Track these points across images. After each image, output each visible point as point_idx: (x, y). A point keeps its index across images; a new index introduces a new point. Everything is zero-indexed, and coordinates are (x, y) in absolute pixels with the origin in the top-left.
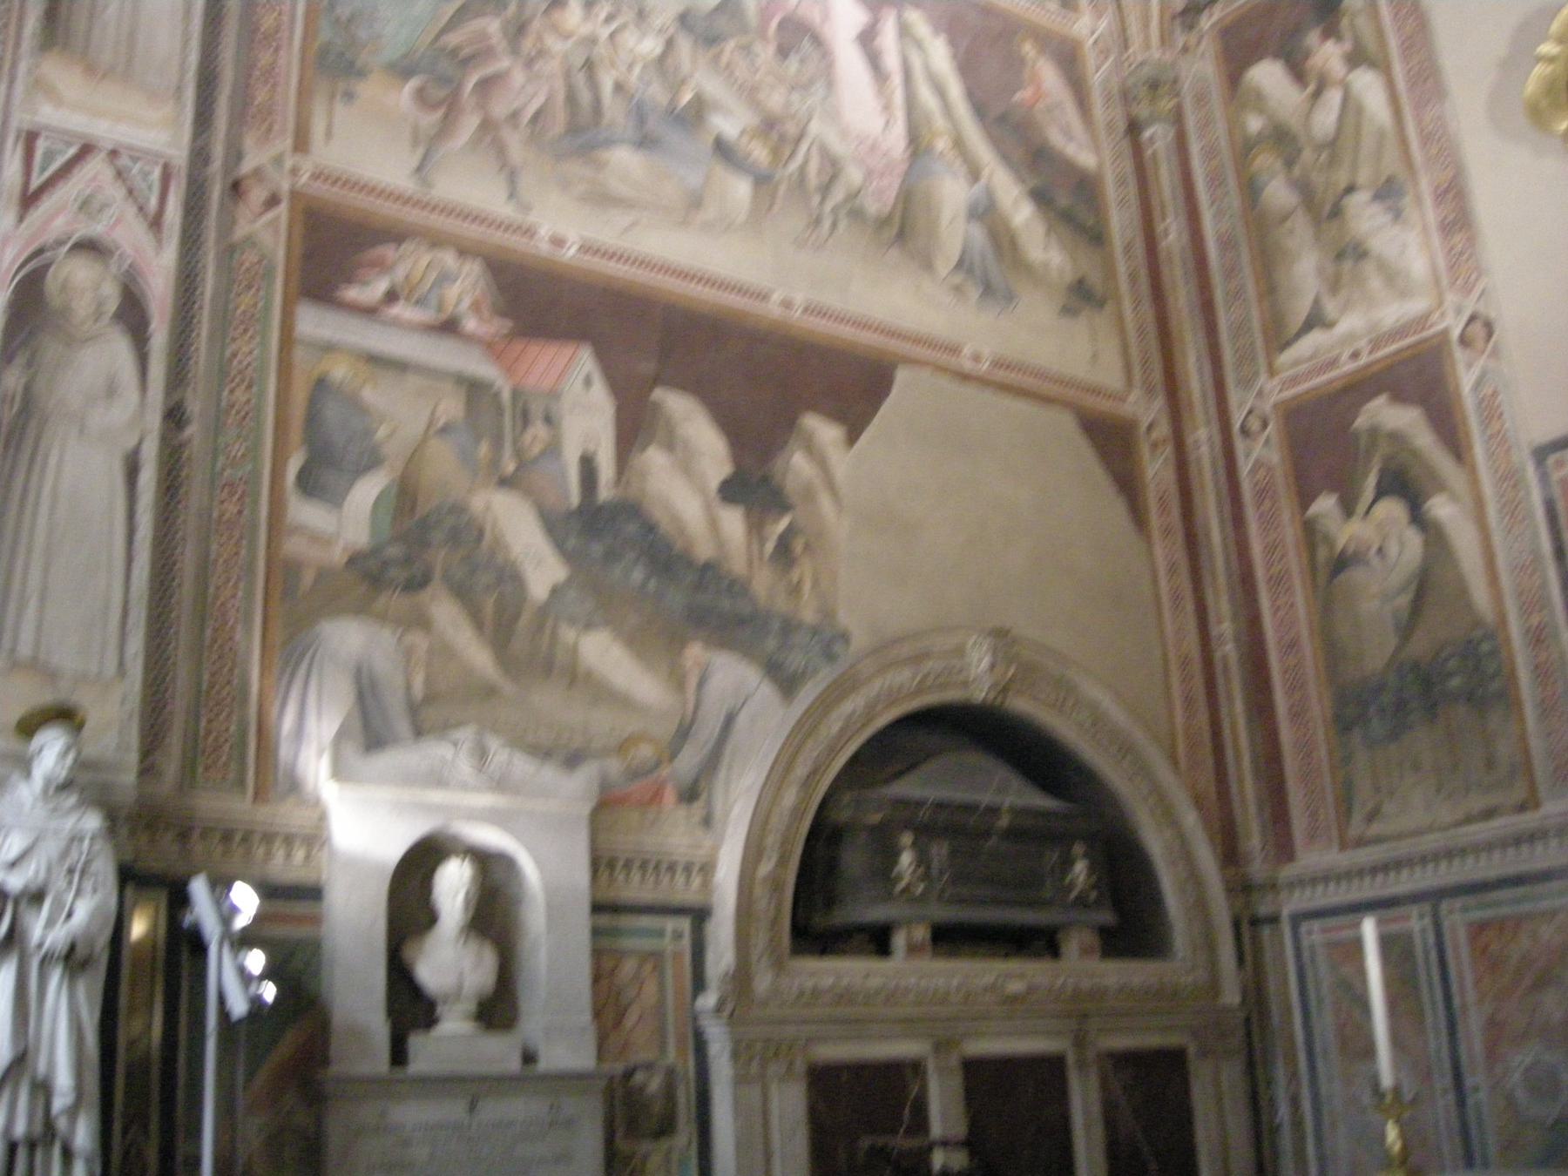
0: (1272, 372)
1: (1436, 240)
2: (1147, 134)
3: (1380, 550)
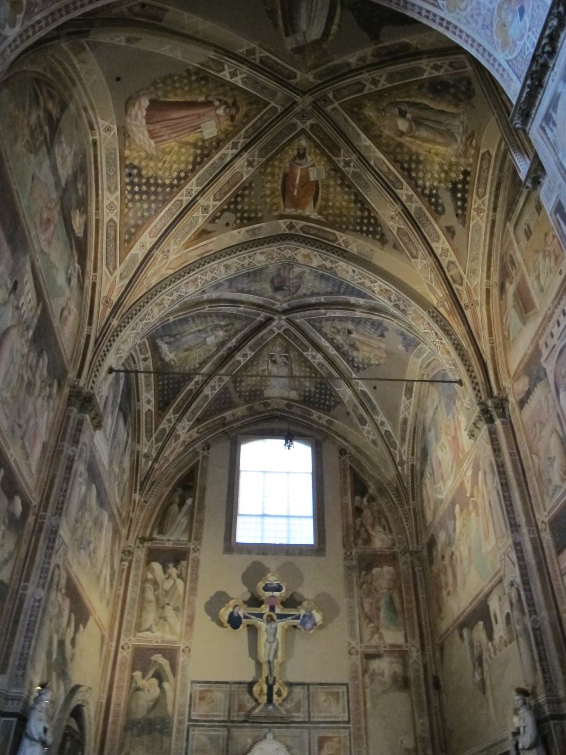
0: (135, 636)
1: (184, 626)
2: (123, 563)
3: (148, 690)
